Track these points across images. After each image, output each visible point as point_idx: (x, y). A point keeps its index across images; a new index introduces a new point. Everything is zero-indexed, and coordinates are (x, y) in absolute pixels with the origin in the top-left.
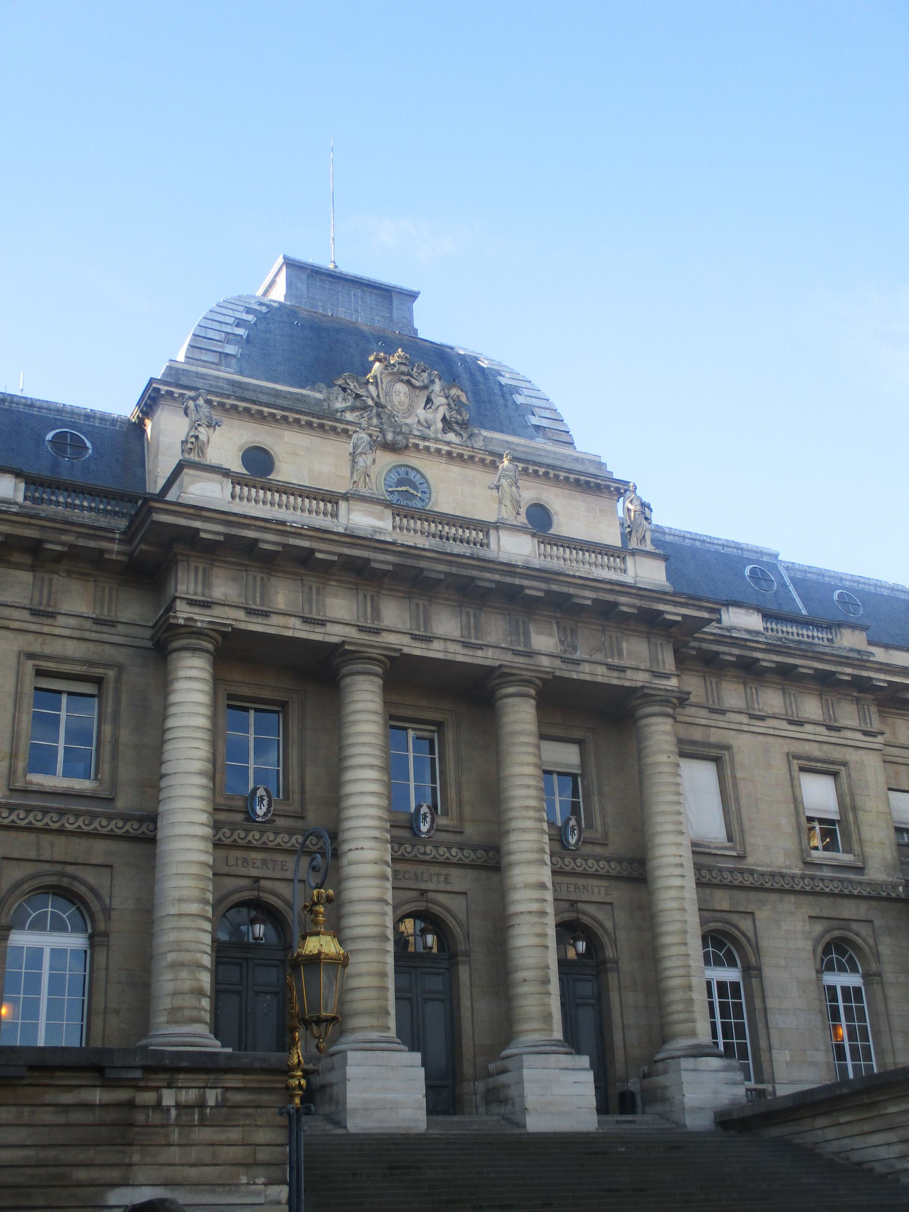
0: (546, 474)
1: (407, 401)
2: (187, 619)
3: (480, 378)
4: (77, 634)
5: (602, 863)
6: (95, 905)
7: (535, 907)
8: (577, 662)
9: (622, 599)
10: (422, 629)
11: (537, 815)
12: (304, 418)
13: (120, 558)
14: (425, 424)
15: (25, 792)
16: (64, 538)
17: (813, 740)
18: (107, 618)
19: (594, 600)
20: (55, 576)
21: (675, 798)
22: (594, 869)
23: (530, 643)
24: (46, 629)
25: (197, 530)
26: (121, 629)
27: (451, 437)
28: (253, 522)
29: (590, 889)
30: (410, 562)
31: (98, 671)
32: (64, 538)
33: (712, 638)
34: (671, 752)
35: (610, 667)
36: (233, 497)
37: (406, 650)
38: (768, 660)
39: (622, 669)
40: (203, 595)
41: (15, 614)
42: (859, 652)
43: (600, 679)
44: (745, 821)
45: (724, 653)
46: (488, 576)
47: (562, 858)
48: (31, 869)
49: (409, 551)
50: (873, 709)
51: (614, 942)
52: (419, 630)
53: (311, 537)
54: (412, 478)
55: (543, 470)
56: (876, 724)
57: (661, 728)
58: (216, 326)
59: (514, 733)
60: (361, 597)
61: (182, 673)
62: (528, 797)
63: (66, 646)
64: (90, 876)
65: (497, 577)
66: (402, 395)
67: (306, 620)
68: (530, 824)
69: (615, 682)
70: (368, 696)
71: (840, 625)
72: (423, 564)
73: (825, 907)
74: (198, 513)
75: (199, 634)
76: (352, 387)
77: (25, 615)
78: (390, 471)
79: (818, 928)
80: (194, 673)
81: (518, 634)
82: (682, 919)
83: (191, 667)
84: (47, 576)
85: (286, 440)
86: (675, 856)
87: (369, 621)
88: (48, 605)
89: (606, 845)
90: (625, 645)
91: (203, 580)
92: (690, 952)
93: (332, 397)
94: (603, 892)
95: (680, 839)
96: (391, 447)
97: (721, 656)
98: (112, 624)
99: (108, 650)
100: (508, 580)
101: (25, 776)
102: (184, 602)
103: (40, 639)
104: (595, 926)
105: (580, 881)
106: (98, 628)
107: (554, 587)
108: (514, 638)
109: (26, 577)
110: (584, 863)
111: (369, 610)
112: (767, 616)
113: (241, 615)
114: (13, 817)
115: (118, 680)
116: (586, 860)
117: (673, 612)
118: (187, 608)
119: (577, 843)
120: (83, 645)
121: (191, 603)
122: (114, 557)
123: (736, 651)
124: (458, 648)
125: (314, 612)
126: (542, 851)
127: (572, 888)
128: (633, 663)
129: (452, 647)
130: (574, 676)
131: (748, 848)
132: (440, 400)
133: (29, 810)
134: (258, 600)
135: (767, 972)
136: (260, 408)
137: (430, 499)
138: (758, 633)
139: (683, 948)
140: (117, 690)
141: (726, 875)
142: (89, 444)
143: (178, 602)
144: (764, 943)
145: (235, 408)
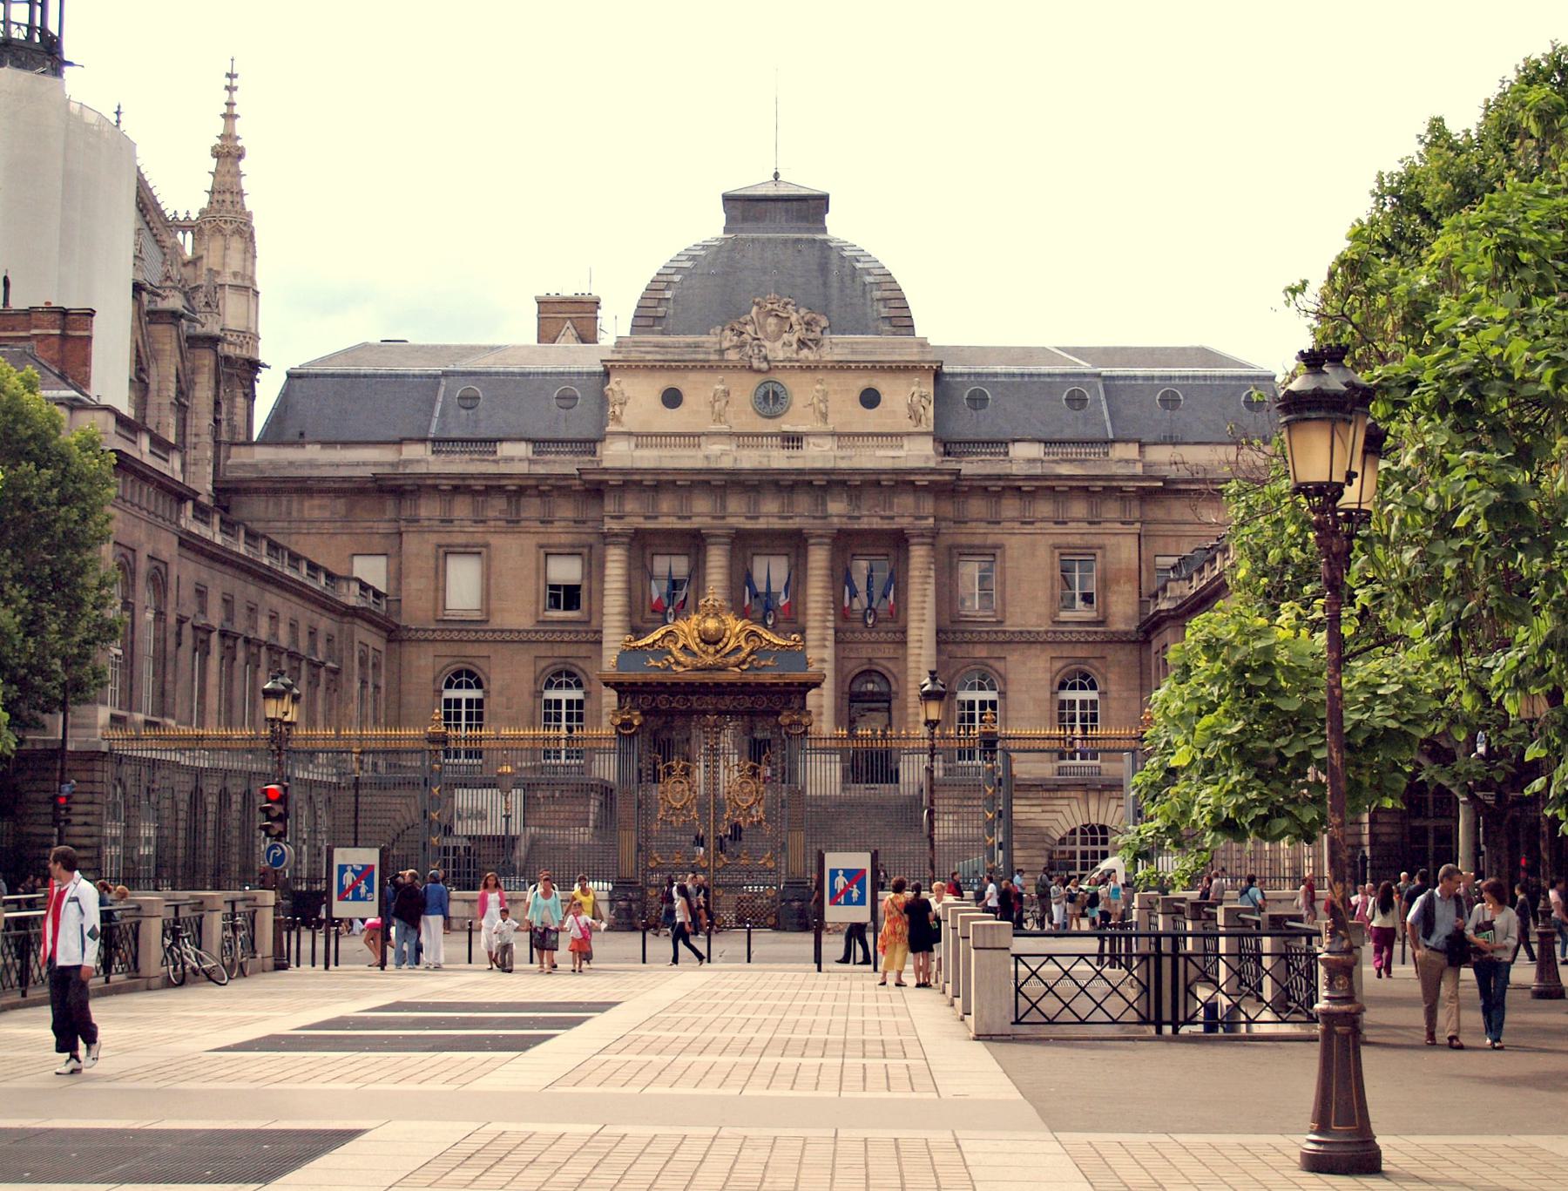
3: (848, 280)
6: (584, 679)
17: (1076, 533)
27: (805, 352)
38: (1027, 486)
39: (892, 518)
41: (531, 524)
42: (1127, 461)
44: (1008, 596)
48: (551, 661)
50: (1135, 503)
56: (1136, 514)
64: (581, 664)
67: (679, 518)
71: (1113, 442)
73: (1067, 651)
75: (616, 535)
79: (1058, 665)
98: (584, 522)
109: (537, 501)
112: (1048, 443)
113: (641, 520)
123: (1001, 483)
124: (776, 520)
126: (825, 639)
132: (796, 327)
135: (1009, 694)
138: (1034, 460)
140: (590, 560)
141: (985, 636)
144: (1011, 676)
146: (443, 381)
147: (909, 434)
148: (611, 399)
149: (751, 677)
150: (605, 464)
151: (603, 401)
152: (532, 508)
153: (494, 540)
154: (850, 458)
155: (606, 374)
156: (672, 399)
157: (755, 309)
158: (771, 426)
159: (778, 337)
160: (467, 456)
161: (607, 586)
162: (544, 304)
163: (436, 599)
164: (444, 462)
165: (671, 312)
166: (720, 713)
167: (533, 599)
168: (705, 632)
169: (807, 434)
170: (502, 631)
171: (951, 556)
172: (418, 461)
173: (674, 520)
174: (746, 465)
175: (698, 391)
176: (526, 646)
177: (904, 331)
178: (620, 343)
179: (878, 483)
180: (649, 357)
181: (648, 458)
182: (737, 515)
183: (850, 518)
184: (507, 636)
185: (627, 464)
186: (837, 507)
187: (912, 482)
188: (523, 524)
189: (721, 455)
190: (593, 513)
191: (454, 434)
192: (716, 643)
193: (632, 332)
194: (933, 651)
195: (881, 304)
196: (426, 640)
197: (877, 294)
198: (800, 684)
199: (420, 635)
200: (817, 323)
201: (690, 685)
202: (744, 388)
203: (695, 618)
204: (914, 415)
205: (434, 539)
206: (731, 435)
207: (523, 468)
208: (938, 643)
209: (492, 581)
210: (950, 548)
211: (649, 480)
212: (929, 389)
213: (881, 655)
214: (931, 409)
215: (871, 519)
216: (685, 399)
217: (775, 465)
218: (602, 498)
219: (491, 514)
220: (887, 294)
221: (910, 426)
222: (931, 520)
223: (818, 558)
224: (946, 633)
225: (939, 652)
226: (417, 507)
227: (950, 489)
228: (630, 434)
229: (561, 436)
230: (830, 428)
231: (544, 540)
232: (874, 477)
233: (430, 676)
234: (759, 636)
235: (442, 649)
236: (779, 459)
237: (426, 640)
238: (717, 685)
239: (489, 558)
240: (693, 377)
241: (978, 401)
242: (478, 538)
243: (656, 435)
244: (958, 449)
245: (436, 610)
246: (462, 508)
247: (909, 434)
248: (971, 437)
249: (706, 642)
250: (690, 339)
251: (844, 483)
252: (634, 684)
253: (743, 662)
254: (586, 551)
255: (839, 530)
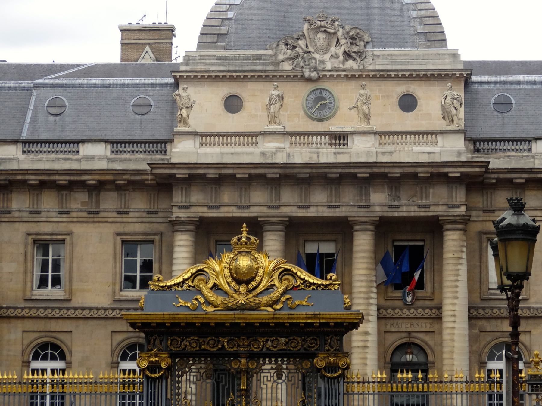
0: (411, 75)
1: (325, 44)
2: (176, 217)
4: (140, 220)
5: (426, 311)
7: (361, 344)
8: (398, 207)
9: (419, 170)
10: (303, 201)
11: (366, 296)
12: (257, 74)
13: (153, 182)
14: (335, 56)
15: (120, 301)
16: (125, 177)
18: (153, 210)
19: (400, 173)
20: (127, 192)
21: (455, 278)
22: (421, 314)
23: (370, 200)
24: (125, 220)
25: (175, 174)
26: (161, 214)
27: (350, 64)
28: (201, 166)
29: (420, 325)
30: (288, 171)
31: (150, 238)
32: (125, 177)
33: (506, 170)
34: (456, 251)
35: (420, 206)
36: (201, 144)
37: (294, 215)
39: (427, 206)
40: (186, 202)
43: (412, 214)
45: (516, 178)
46: (335, 170)
47: (401, 309)
48: (125, 336)
49: (285, 166)
51: (433, 351)
52: (301, 202)
53: (233, 167)
54: (324, 95)
55: (409, 73)
57: (451, 237)
58: (217, 15)
59: (357, 252)
60: (269, 189)
61: (177, 243)
62: (361, 287)
63: (135, 227)
65: (340, 170)
66: (322, 40)
67: (239, 207)
68: (361, 301)
69: (422, 214)
70: (271, 243)
72: (296, 171)
74: (173, 166)
76: (290, 42)
77: (115, 214)
78: (310, 93)
80: (182, 243)
81: (361, 195)
82: (451, 345)
83: (181, 240)
84: (123, 193)
85: (249, 87)
86: (451, 310)
87: (274, 202)
88: (125, 208)
89: (433, 299)
90: (431, 191)
91: (186, 194)
92: (455, 363)
93: (278, 52)
94: (428, 325)
95: (456, 301)
96: (310, 80)
97: (514, 180)
98: (156, 212)
99: (156, 226)
100: (347, 171)
101: (119, 293)
102: (176, 208)
103: (123, 225)
104: (422, 344)
105: (414, 321)
106: (150, 216)
107: (376, 170)
108: (359, 198)
109: (114, 194)
110: (415, 311)
111: (273, 196)
113: (205, 209)
114: (114, 313)
115: (161, 241)
116: (416, 309)
117: (454, 172)
118: (178, 210)
119: (412, 300)
120: (143, 225)
121: (180, 207)
122: (149, 182)
123: (526, 176)
124: (325, 209)
125: (243, 201)
127: (409, 325)
128: (436, 201)
129: (321, 209)
130: (396, 214)
131: (531, 293)
132: (343, 41)
133: (121, 309)
134: (213, 200)
136: (231, 74)
137: (334, 107)
139: (451, 360)
140: (161, 246)
142: (152, 103)
143: (174, 208)
145: (216, 76)
146: (35, 92)
147: (442, 132)
148: (179, 103)
149: (284, 317)
150: (173, 161)
151: (174, 106)
152: (109, 201)
153: (77, 229)
154: (391, 153)
155: (176, 85)
156: (233, 104)
157: (306, 26)
158: (320, 127)
159: (326, 50)
160: (53, 156)
161: (175, 268)
162: (124, 31)
163: (25, 281)
164: (33, 160)
165: (233, 30)
166: (252, 356)
167: (111, 280)
168: (237, 270)
169: (352, 133)
170: (83, 309)
171: (480, 241)
172: (10, 160)
173: (234, 209)
174: (298, 160)
175: (256, 98)
176: (102, 322)
177: (437, 44)
178: (188, 59)
179: (415, 176)
180: (213, 68)
181: (211, 154)
182: (291, 204)
183: (390, 206)
184: (87, 313)
185: (193, 160)
186: (379, 198)
187: (446, 174)
188: (102, 214)
189: (276, 151)
190: (163, 205)
191: (43, 137)
192: (248, 282)
193: (199, 47)
194: (466, 325)
195: (417, 22)
196: (16, 317)
197: (414, 14)
198: (337, 324)
199: (11, 312)
200: (361, 39)
201: (220, 325)
202: (296, 95)
203: (227, 257)
204: (447, 116)
205: (23, 228)
206: (284, 134)
207: (102, 165)
208: (470, 318)
209: (75, 265)
210: (480, 233)
211: (212, 174)
212: (459, 91)
213: (419, 329)
214: (462, 110)
215: (408, 209)
216: (246, 104)
217: (323, 160)
218: (172, 192)
219: (75, 206)
220: (423, 12)
221: (442, 125)
222: (463, 208)
223: (363, 243)
224: (476, 308)
225: (471, 327)
226: (9, 200)
227: (477, 181)
228: (195, 134)
229: (137, 137)
230: (371, 128)
231: (121, 228)
232: (411, 170)
233: (19, 348)
234: (294, 275)
235: (29, 325)
236: (327, 154)
237: (16, 317)
238: (250, 325)
239: (72, 245)
240: (252, 86)
241: (503, 105)
242: (62, 228)
243: (219, 135)
244: (486, 146)
245: (24, 290)
246: (49, 202)
247: (442, 132)
248: (497, 136)
249: (239, 282)
250: (249, 53)
251: (384, 176)
252: (161, 325)
253: (277, 302)
254: (157, 238)
255: (381, 218)
